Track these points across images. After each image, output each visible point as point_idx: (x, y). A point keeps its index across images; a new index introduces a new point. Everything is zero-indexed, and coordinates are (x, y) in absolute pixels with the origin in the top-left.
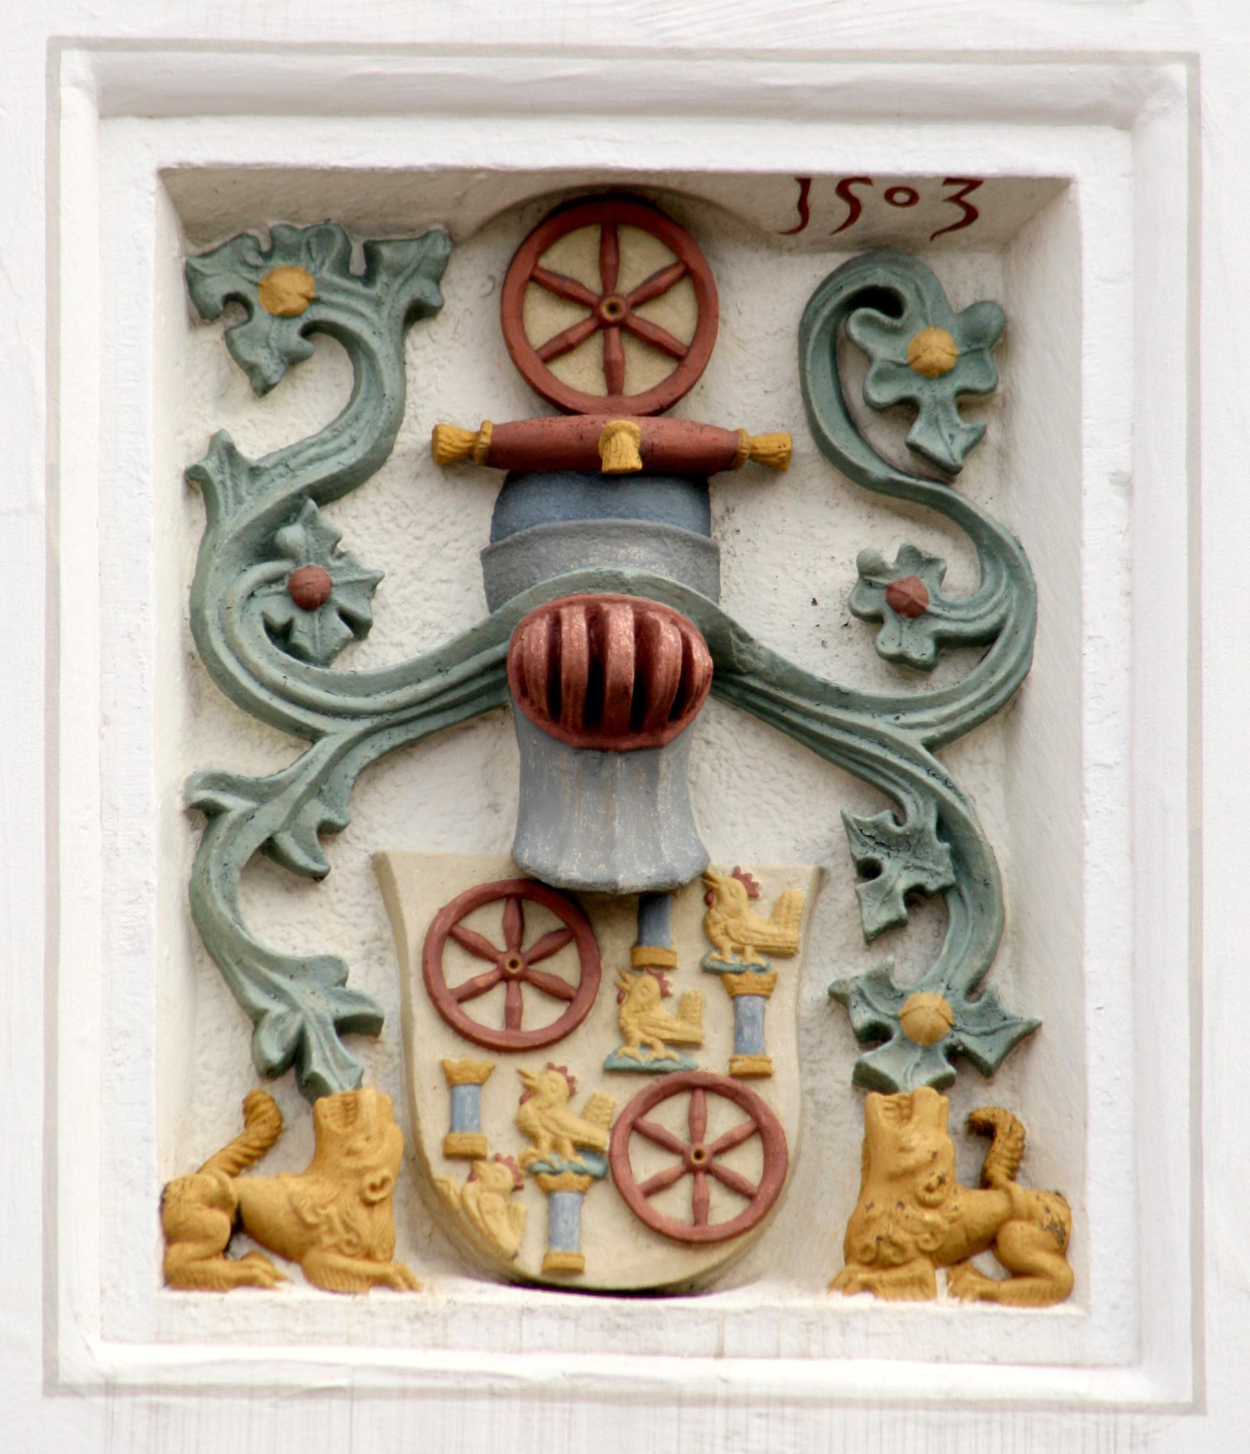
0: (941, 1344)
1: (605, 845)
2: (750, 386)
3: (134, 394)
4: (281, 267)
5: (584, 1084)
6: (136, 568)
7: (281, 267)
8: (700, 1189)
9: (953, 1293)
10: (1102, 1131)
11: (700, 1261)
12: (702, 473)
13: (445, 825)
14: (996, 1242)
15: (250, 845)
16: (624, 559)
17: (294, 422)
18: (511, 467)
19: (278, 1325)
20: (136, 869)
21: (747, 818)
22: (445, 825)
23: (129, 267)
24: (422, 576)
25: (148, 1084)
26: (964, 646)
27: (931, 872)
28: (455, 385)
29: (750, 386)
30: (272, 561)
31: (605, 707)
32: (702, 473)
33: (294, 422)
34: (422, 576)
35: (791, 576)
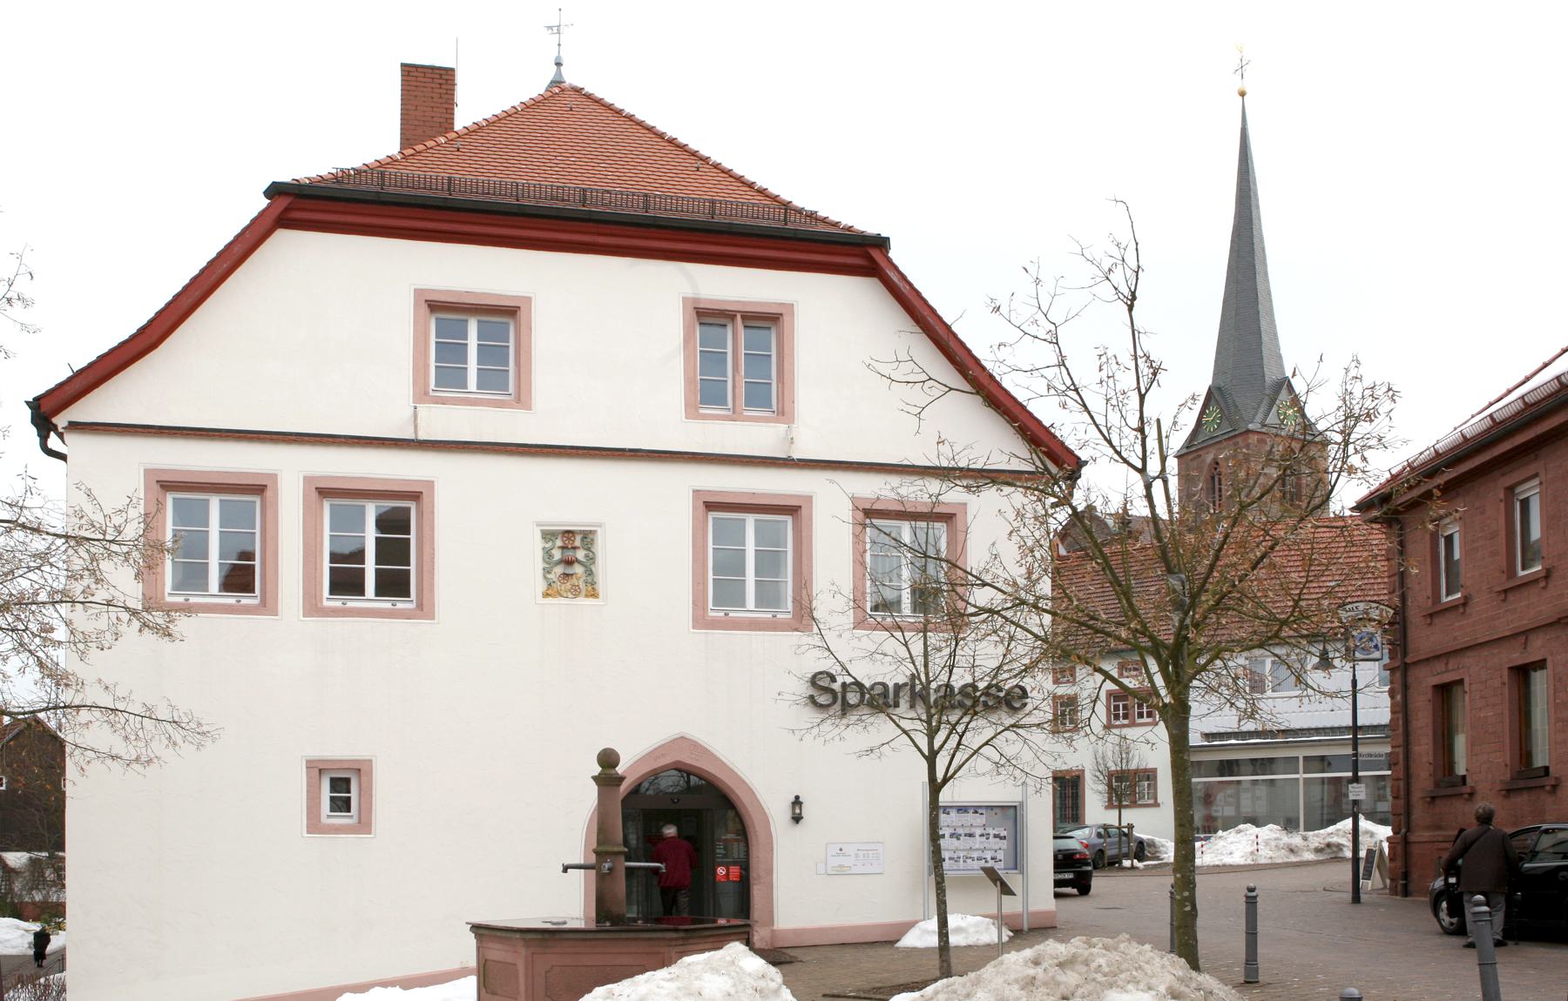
0: (591, 601)
1: (569, 571)
2: (578, 543)
3: (539, 544)
4: (548, 535)
5: (568, 585)
6: (539, 554)
7: (548, 535)
8: (576, 592)
9: (62, 970)
10: (600, 587)
11: (576, 596)
12: (575, 548)
13: (559, 570)
14: (594, 595)
15: (547, 571)
16: (570, 554)
17: (549, 545)
18: (563, 548)
19: (549, 600)
20: (540, 572)
21: (578, 569)
22: (559, 570)
23: (539, 536)
24: (557, 555)
25: (541, 586)
26: (591, 559)
27: (590, 573)
28: (559, 543)
29: (578, 543)
30: (548, 554)
31: (569, 563)
32: (575, 548)
33: (549, 545)
34: (557, 555)
35: (580, 554)
